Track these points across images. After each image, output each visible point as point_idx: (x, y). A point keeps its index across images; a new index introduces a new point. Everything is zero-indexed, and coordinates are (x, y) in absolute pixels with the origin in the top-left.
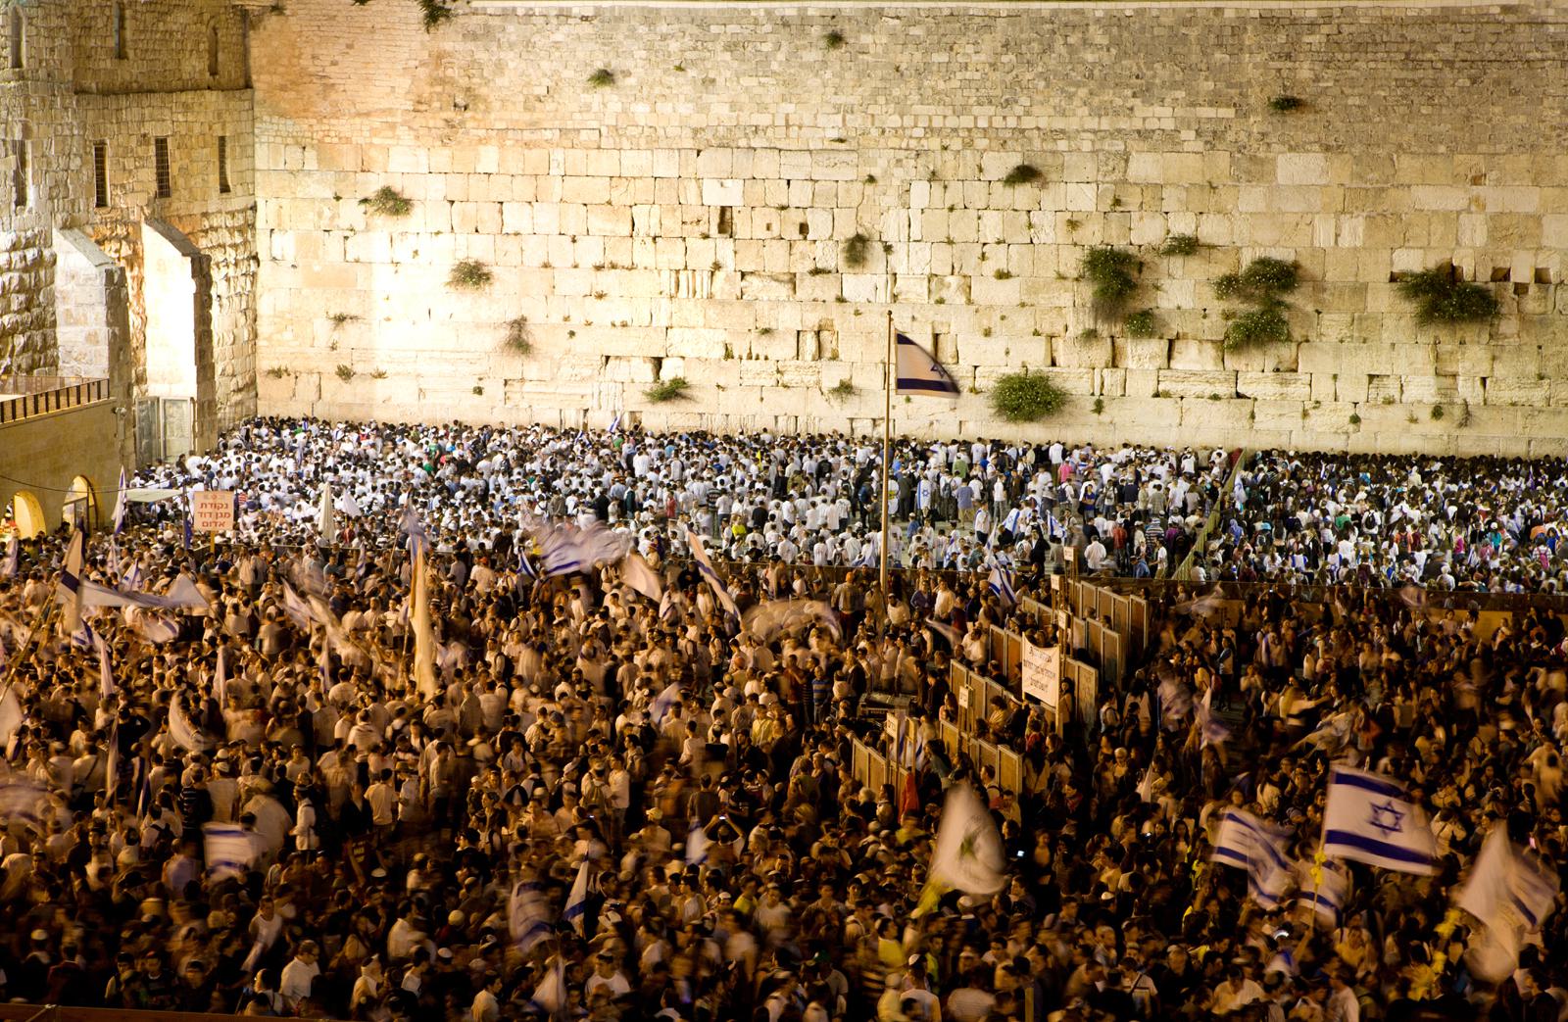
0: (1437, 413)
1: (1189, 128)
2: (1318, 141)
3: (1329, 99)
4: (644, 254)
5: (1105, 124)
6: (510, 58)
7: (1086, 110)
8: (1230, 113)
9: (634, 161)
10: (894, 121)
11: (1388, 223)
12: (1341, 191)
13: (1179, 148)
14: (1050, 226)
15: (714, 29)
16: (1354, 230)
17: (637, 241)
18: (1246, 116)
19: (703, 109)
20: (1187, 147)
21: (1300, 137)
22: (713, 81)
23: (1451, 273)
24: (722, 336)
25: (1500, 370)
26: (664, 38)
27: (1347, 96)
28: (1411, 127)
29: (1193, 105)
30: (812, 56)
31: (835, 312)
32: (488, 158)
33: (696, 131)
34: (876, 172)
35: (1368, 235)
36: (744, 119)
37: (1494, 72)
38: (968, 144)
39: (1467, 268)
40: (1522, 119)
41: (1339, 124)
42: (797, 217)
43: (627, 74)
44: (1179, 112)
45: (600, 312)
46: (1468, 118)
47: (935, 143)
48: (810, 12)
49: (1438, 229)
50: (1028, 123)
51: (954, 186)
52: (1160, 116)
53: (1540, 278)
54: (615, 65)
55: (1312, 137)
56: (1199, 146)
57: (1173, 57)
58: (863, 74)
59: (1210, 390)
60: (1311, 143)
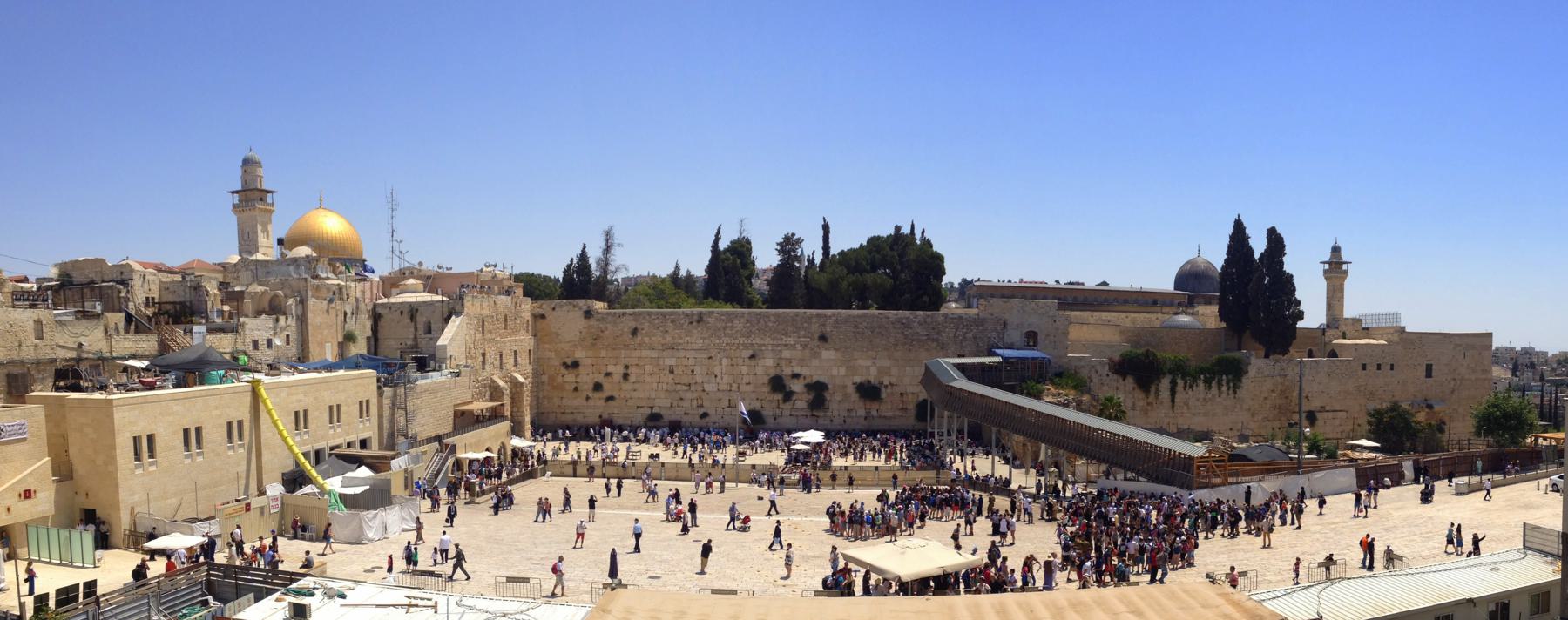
7: (769, 339)
9: (645, 353)
10: (718, 341)
14: (760, 370)
15: (668, 317)
16: (843, 371)
17: (646, 376)
19: (665, 339)
22: (667, 331)
23: (869, 382)
24: (669, 401)
26: (654, 319)
29: (799, 337)
31: (702, 394)
32: (603, 353)
36: (676, 341)
37: (877, 330)
38: (738, 348)
39: (872, 381)
40: (884, 342)
43: (643, 329)
44: (796, 339)
45: (635, 395)
48: (695, 312)
50: (754, 342)
51: (734, 359)
52: (790, 340)
53: (891, 384)
54: (639, 327)
58: (708, 329)
59: (805, 414)
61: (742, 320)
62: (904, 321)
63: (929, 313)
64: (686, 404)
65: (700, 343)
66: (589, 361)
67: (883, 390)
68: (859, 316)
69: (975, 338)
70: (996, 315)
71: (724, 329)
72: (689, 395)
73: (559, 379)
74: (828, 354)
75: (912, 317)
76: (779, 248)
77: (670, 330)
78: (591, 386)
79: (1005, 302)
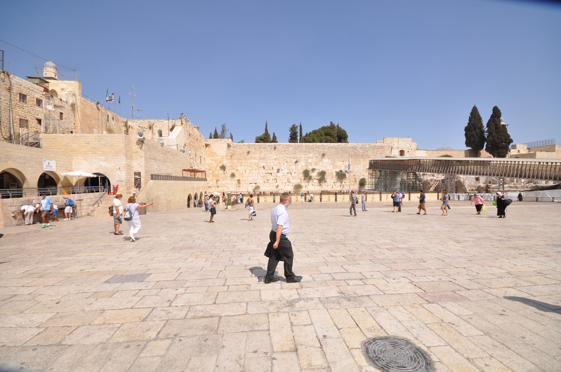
0: (340, 186)
4: (254, 172)
5: (305, 156)
6: (238, 150)
8: (318, 155)
9: (253, 161)
10: (282, 156)
11: (335, 166)
16: (331, 166)
30: (273, 149)
32: (235, 161)
33: (260, 157)
34: (280, 162)
38: (291, 158)
42: (272, 167)
43: (252, 151)
47: (287, 158)
50: (297, 156)
52: (311, 155)
57: (312, 149)
58: (279, 151)
61: (292, 148)
62: (354, 147)
63: (363, 144)
64: (270, 182)
65: (275, 157)
66: (229, 165)
67: (347, 174)
68: (337, 146)
69: (381, 153)
70: (388, 144)
71: (285, 151)
72: (271, 178)
73: (216, 173)
74: (325, 160)
75: (357, 146)
76: (290, 129)
77: (263, 151)
78: (230, 174)
79: (391, 139)
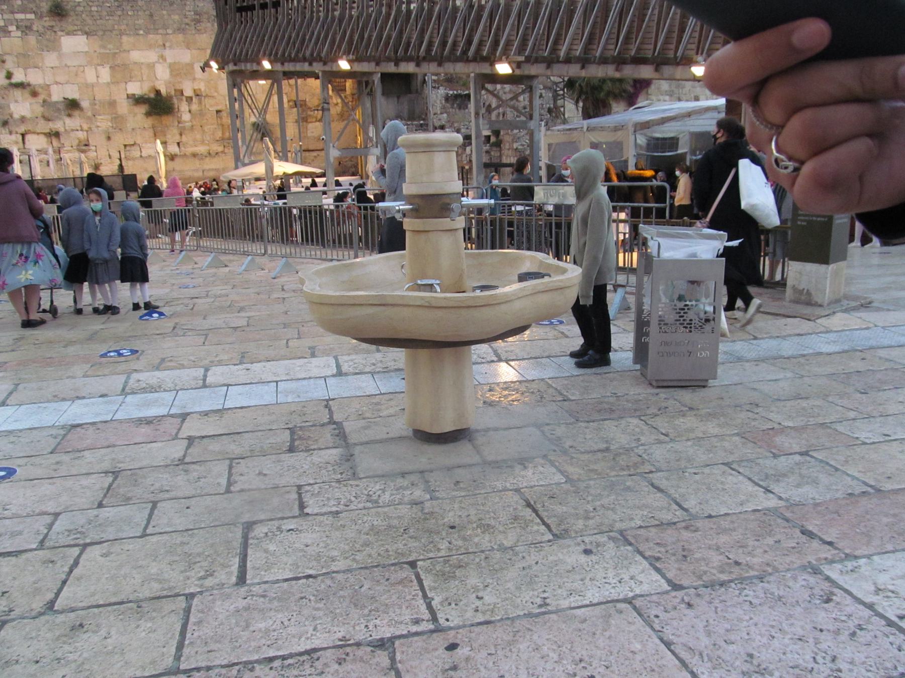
1: (12, 25)
2: (81, 30)
3: (81, 9)
8: (32, 16)
12: (96, 54)
13: (8, 35)
16: (105, 74)
18: (41, 17)
20: (12, 34)
21: (71, 28)
23: (158, 93)
25: (184, 138)
27: (91, 6)
28: (125, 22)
29: (13, 13)
35: (112, 76)
41: (90, 22)
46: (151, 15)
49: (145, 71)
55: (76, 28)
56: (19, 34)
60: (75, 31)
67: (184, 107)
